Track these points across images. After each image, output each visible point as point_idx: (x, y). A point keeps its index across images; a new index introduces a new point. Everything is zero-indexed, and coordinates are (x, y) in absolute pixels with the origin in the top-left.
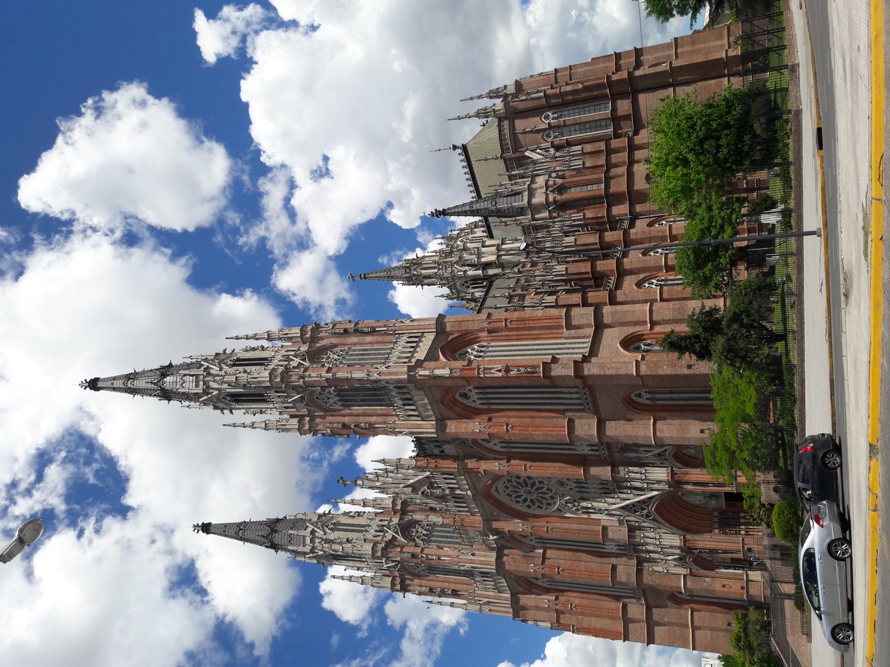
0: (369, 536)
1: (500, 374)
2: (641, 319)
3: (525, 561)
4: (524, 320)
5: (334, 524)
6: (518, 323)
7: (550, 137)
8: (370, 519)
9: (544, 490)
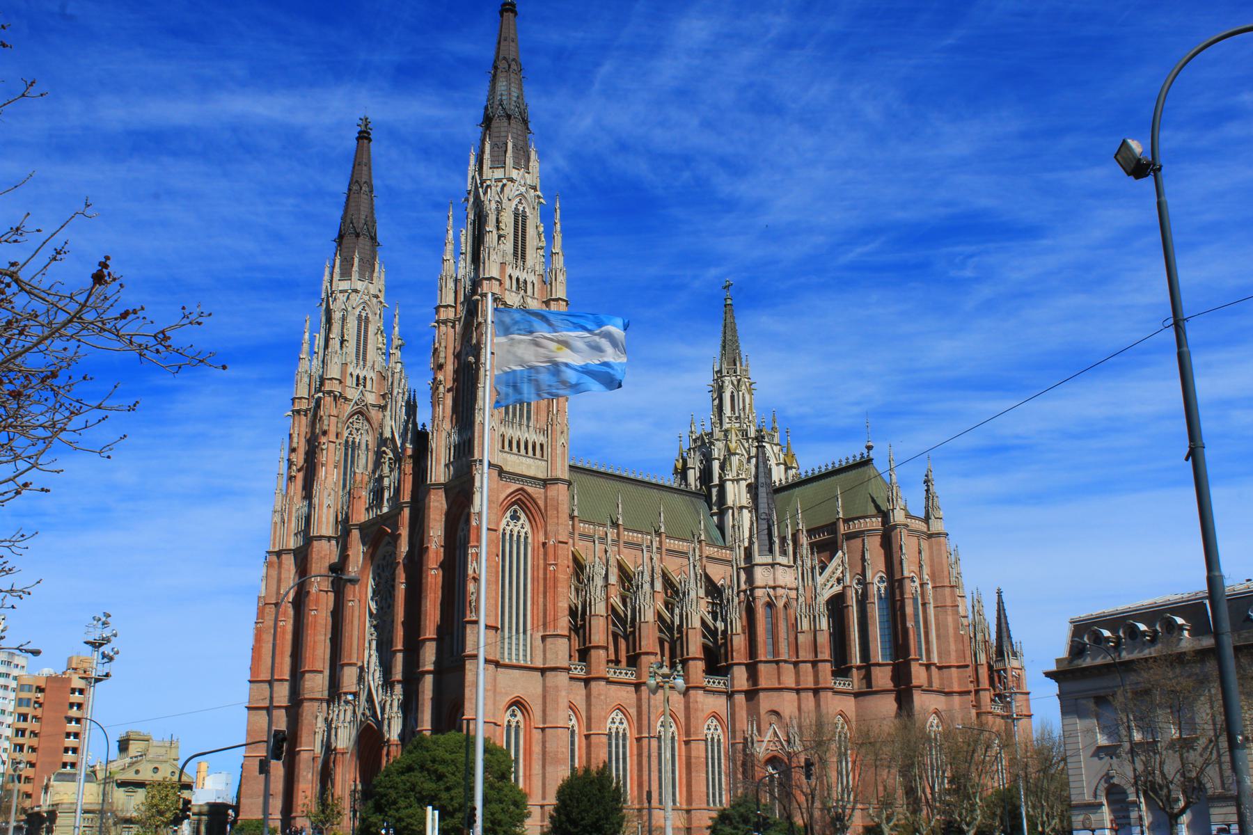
0: (350, 369)
1: (470, 572)
2: (548, 718)
4: (555, 587)
5: (367, 318)
6: (552, 579)
8: (374, 365)
9: (389, 600)
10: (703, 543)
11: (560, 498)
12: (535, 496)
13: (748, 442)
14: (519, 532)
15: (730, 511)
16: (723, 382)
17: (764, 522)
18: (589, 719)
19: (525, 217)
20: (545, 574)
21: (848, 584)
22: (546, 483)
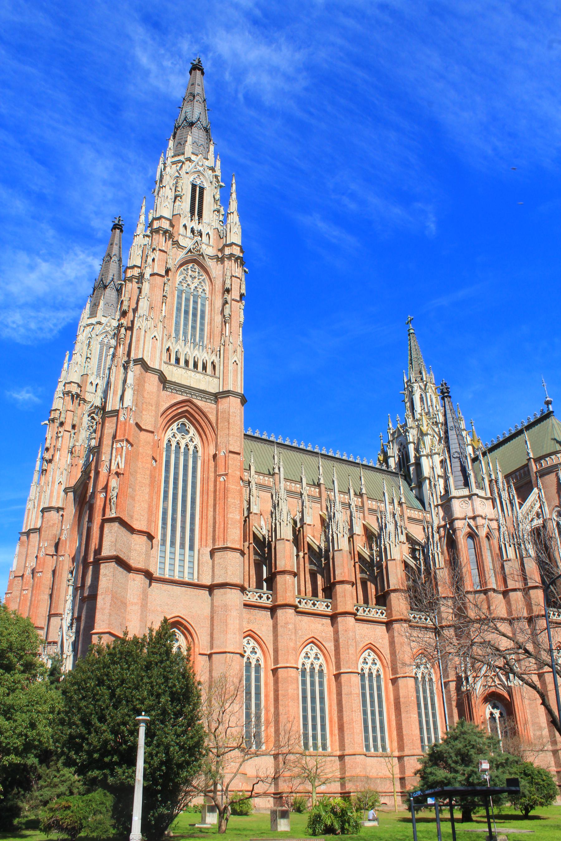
0: (91, 379)
3: (50, 536)
4: (225, 497)
6: (222, 491)
7: (557, 516)
10: (404, 505)
11: (231, 411)
12: (205, 410)
13: (437, 427)
14: (187, 445)
15: (427, 481)
16: (412, 387)
17: (457, 460)
18: (276, 651)
19: (202, 190)
20: (215, 486)
21: (548, 516)
22: (217, 397)
